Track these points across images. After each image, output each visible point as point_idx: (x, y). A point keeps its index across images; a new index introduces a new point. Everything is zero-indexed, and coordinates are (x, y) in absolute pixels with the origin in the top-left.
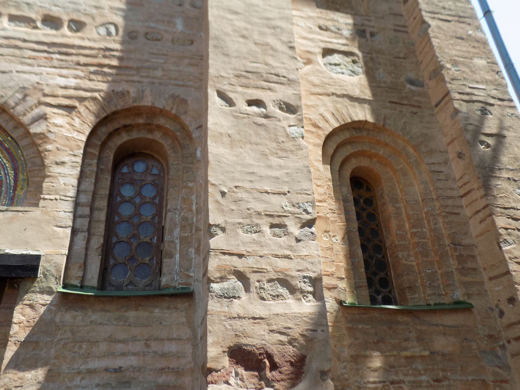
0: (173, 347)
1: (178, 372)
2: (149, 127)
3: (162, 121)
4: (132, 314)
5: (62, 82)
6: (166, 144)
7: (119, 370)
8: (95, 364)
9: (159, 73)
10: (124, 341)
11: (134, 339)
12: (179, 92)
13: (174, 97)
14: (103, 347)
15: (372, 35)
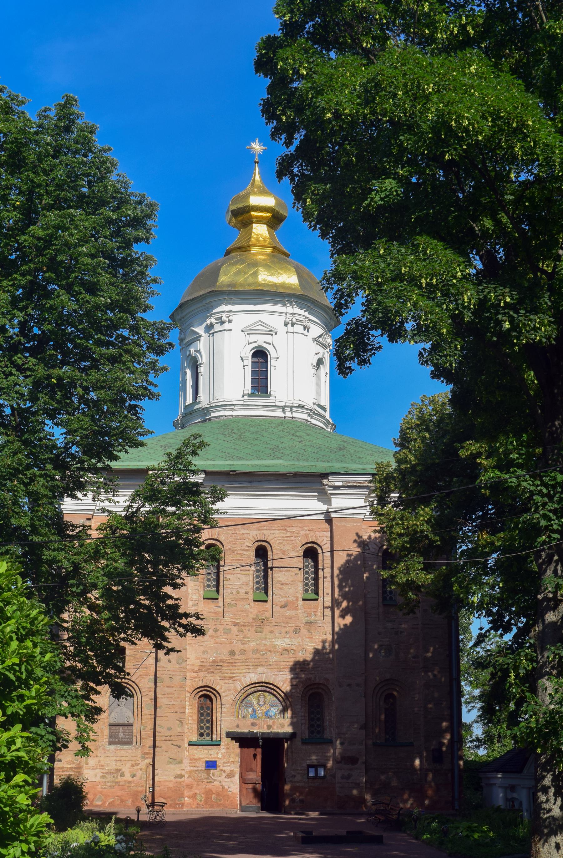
9: (320, 669)
15: (401, 632)
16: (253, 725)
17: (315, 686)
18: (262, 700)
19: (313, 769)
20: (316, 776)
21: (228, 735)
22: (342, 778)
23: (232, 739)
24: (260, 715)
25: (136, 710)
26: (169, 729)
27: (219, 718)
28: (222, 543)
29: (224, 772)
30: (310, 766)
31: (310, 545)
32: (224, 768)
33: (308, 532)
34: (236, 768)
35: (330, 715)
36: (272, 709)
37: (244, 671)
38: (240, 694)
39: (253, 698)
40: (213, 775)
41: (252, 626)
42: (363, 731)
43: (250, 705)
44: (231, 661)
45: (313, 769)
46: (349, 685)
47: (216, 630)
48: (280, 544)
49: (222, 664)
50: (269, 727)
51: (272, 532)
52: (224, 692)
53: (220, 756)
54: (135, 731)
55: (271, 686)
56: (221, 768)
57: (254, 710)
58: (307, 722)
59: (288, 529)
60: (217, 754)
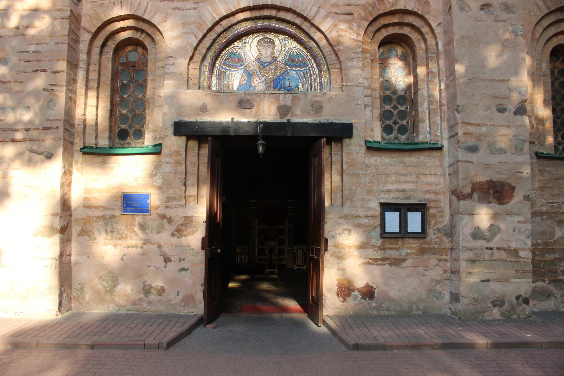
0: (433, 179)
1: (436, 193)
2: (401, 24)
3: (410, 19)
7: (404, 191)
8: (390, 187)
10: (404, 175)
11: (410, 174)
14: (394, 178)
17: (395, 20)
20: (403, 233)
21: (181, 128)
23: (189, 138)
29: (170, 220)
36: (293, 73)
38: (212, 35)
55: (289, 17)
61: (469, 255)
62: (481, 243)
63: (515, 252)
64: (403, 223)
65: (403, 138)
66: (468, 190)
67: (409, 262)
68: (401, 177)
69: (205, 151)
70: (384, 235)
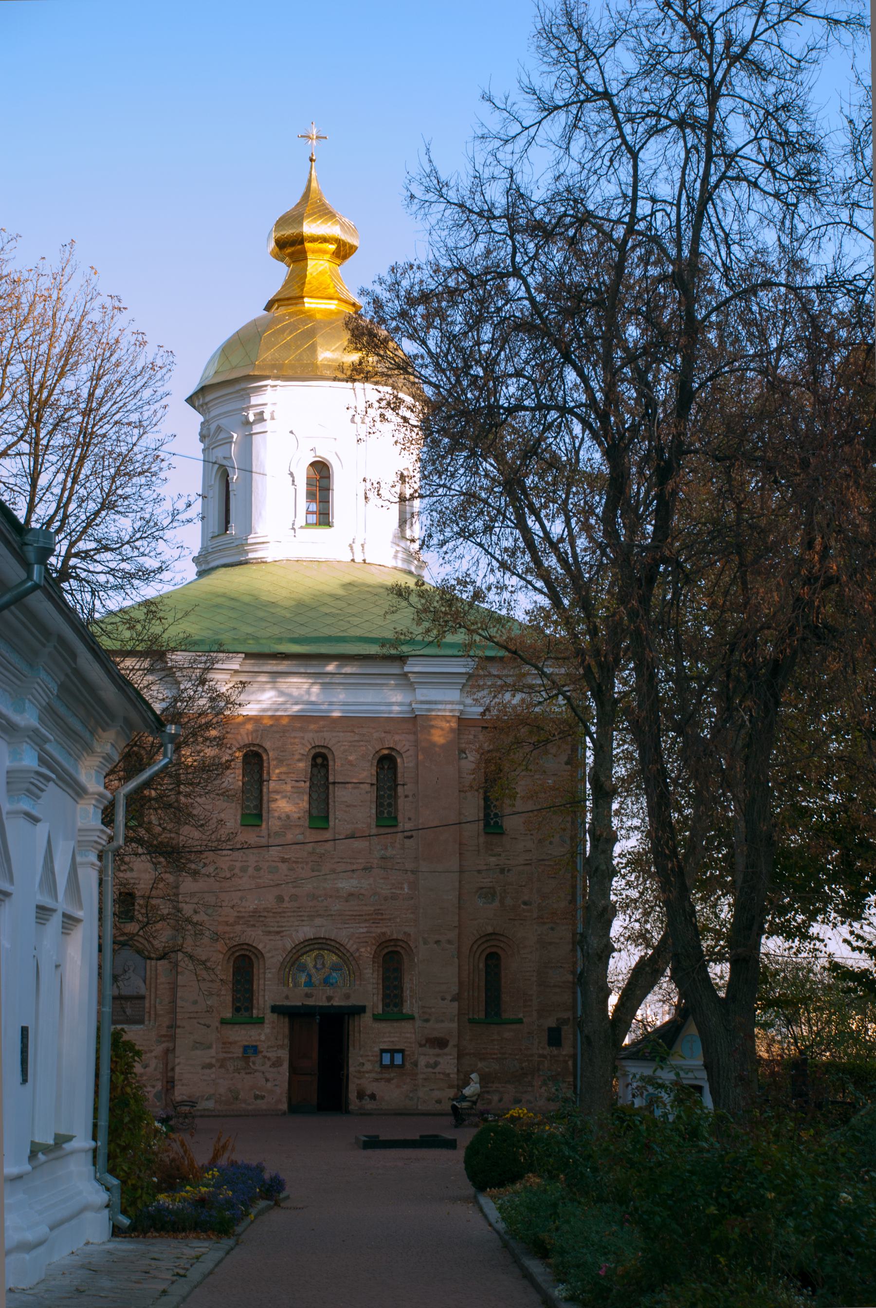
2: (396, 946)
3: (401, 943)
4: (395, 1024)
5: (362, 930)
6: (402, 952)
12: (407, 929)
13: (405, 933)
15: (509, 870)
16: (307, 995)
18: (319, 962)
19: (389, 1055)
20: (392, 1064)
21: (275, 1009)
22: (428, 1066)
24: (317, 983)
25: (148, 976)
26: (195, 1002)
27: (261, 987)
28: (265, 750)
29: (269, 1059)
30: (383, 1051)
31: (386, 752)
32: (269, 1055)
33: (383, 735)
34: (284, 1054)
35: (411, 983)
36: (334, 974)
37: (297, 923)
39: (308, 960)
40: (254, 1063)
41: (307, 863)
42: (456, 1004)
43: (303, 968)
44: (279, 910)
45: (389, 1055)
46: (437, 942)
47: (258, 869)
48: (345, 751)
49: (266, 914)
50: (329, 999)
51: (335, 734)
52: (269, 952)
53: (263, 1038)
54: (147, 1005)
55: (333, 943)
56: (265, 1053)
57: (310, 976)
58: (381, 992)
59: (356, 730)
60: (260, 1034)
61: (421, 1076)
62: (430, 1070)
63: (448, 1074)
64: (392, 1059)
65: (395, 1010)
66: (424, 1042)
67: (395, 1081)
68: (391, 1035)
69: (287, 1020)
70: (382, 1066)
